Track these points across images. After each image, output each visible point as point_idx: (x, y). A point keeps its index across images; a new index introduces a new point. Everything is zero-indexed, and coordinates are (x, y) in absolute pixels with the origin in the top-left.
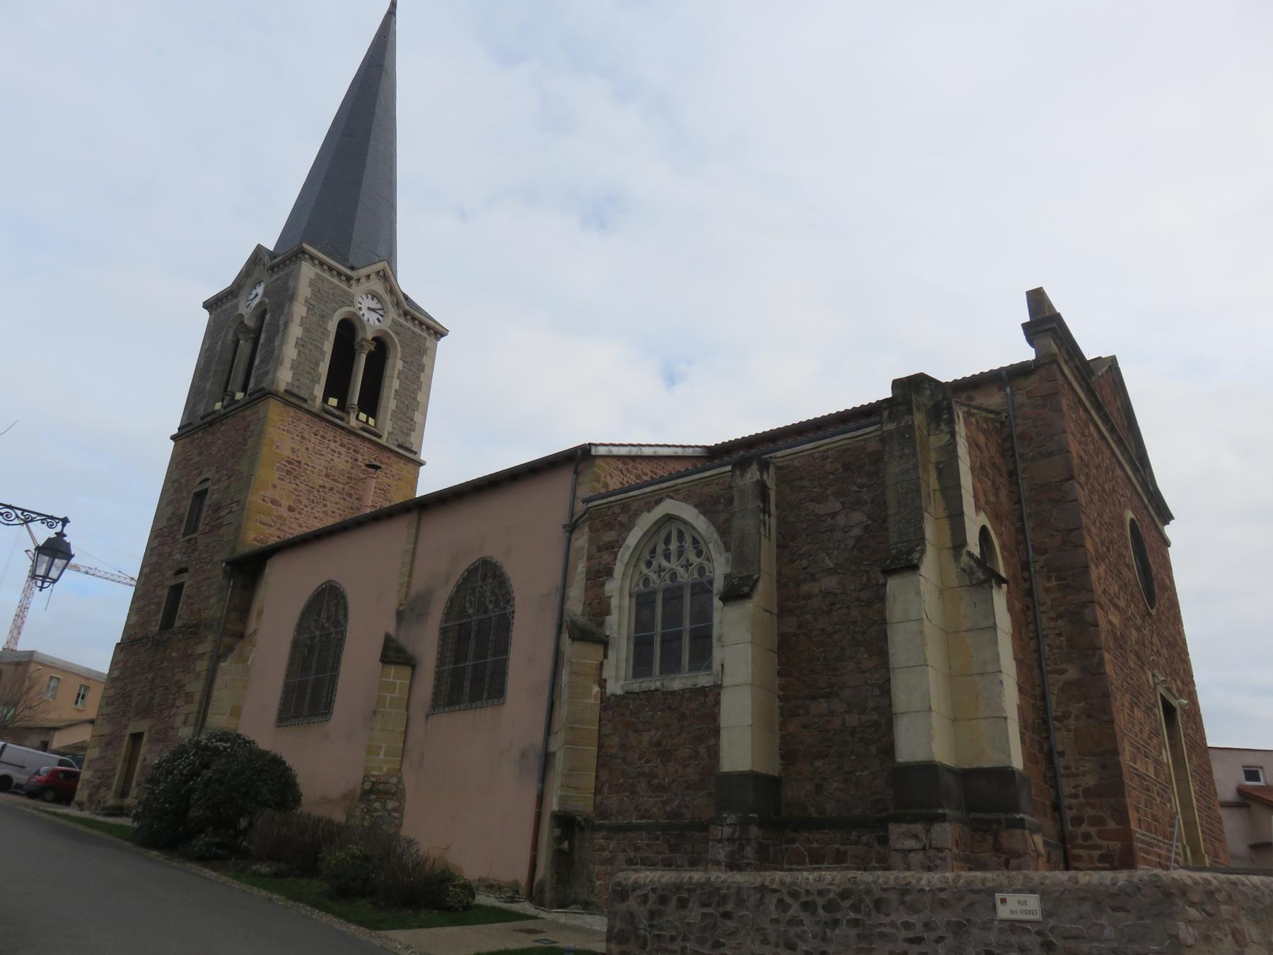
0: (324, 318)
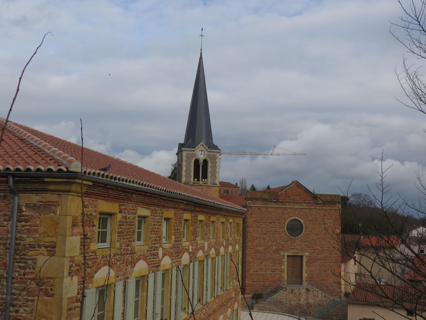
0: (190, 162)
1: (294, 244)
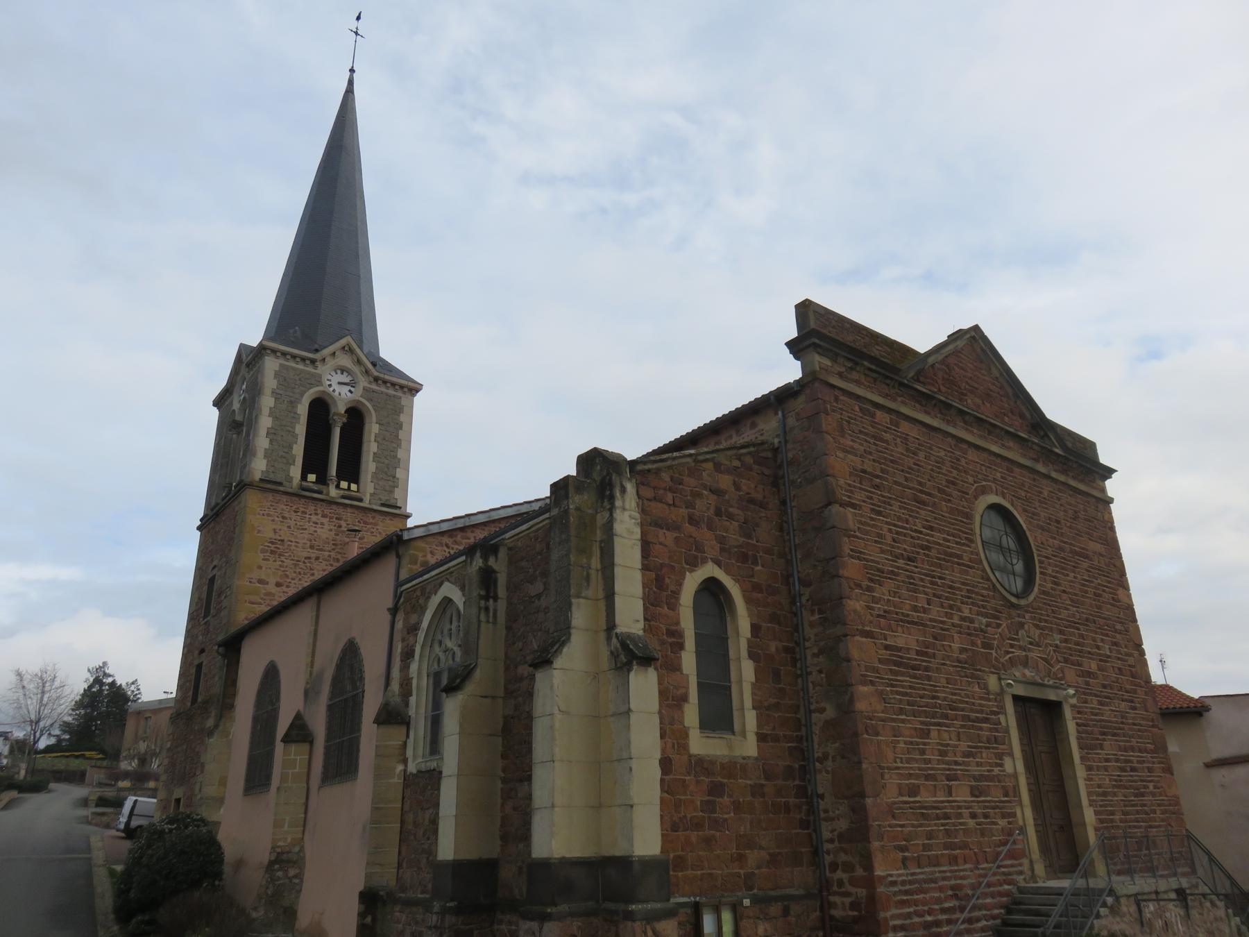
0: (293, 403)
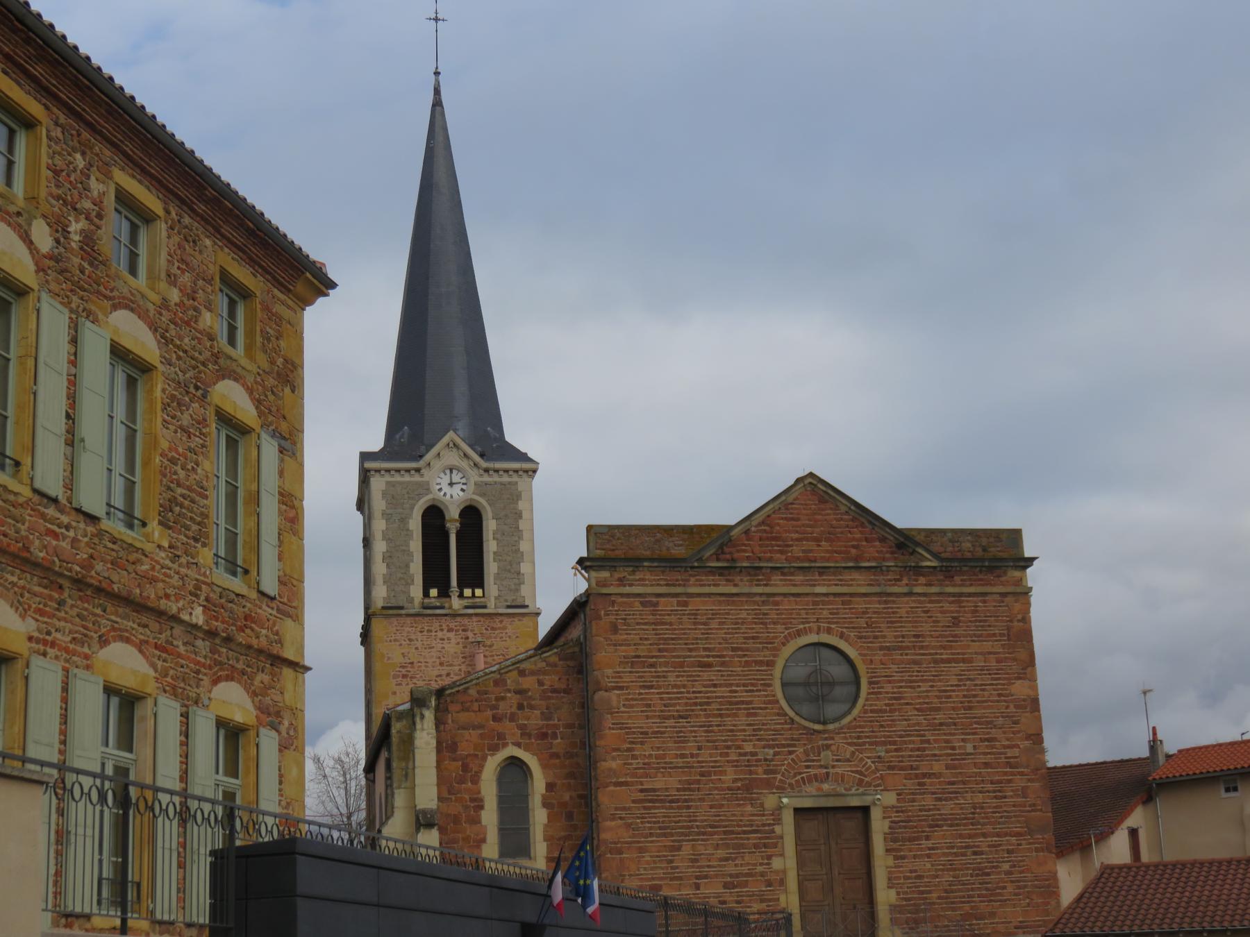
0: (404, 520)
1: (822, 754)
